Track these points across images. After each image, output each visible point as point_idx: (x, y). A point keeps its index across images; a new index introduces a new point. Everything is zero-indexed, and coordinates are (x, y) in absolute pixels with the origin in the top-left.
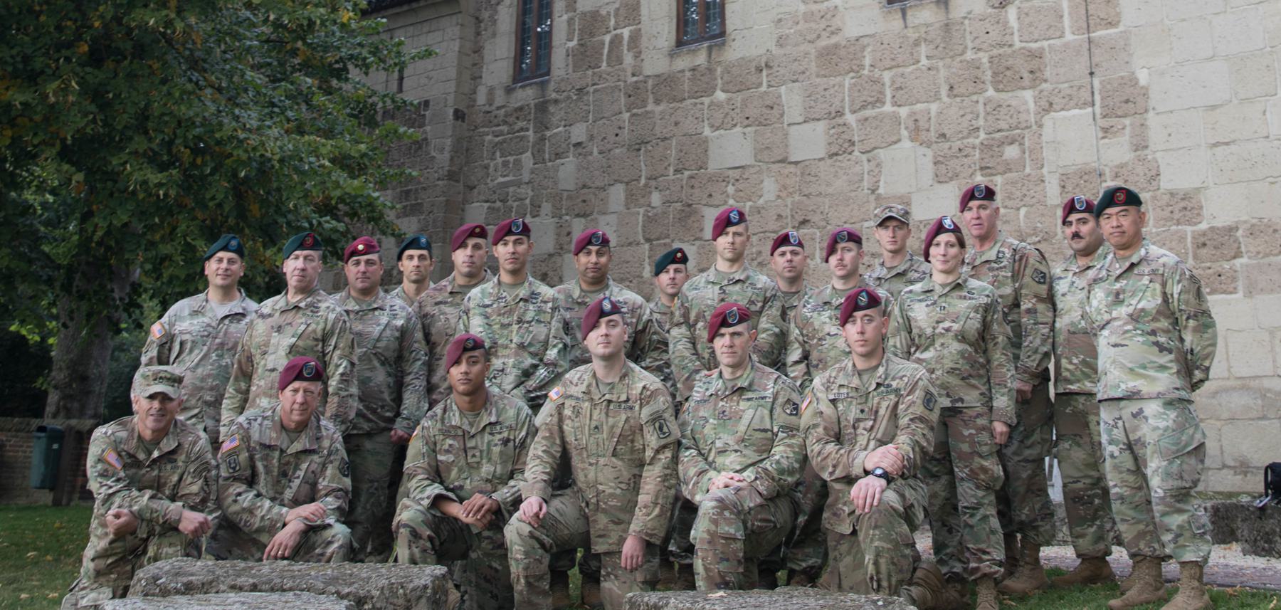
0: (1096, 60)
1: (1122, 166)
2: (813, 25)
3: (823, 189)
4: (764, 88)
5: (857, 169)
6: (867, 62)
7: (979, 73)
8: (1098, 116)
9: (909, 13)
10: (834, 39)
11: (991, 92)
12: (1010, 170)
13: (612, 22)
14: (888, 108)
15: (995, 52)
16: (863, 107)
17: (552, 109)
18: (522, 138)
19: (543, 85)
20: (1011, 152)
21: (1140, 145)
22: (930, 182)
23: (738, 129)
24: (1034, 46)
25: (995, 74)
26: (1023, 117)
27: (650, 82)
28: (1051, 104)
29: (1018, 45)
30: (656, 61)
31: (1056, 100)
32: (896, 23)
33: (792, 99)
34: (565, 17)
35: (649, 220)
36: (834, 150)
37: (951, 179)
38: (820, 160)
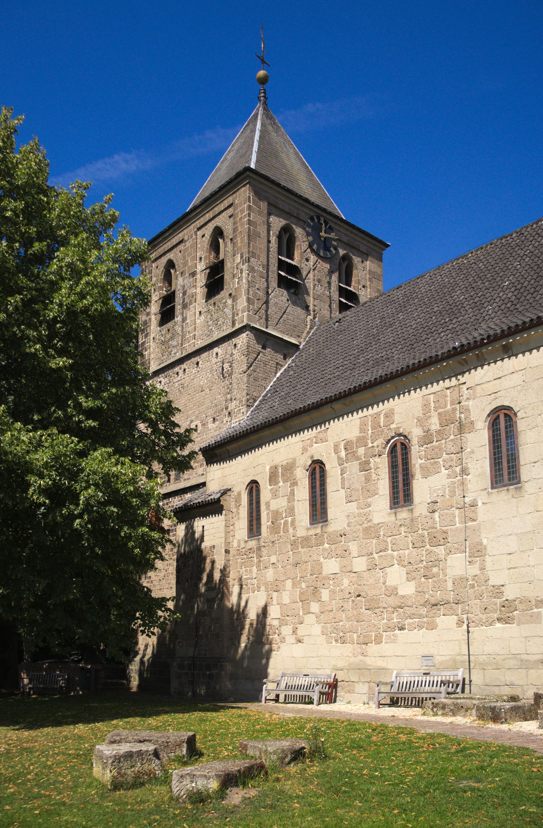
0: (467, 534)
1: (476, 576)
3: (365, 583)
4: (343, 543)
5: (378, 575)
6: (382, 533)
8: (467, 557)
10: (369, 524)
11: (428, 546)
13: (284, 515)
14: (390, 552)
15: (430, 531)
16: (381, 551)
17: (263, 549)
18: (252, 561)
19: (259, 539)
20: (435, 570)
21: (482, 569)
23: (333, 559)
24: (444, 528)
25: (430, 539)
26: (440, 556)
27: (300, 540)
29: (439, 528)
30: (301, 533)
31: (452, 550)
32: (393, 518)
34: (266, 512)
35: (301, 594)
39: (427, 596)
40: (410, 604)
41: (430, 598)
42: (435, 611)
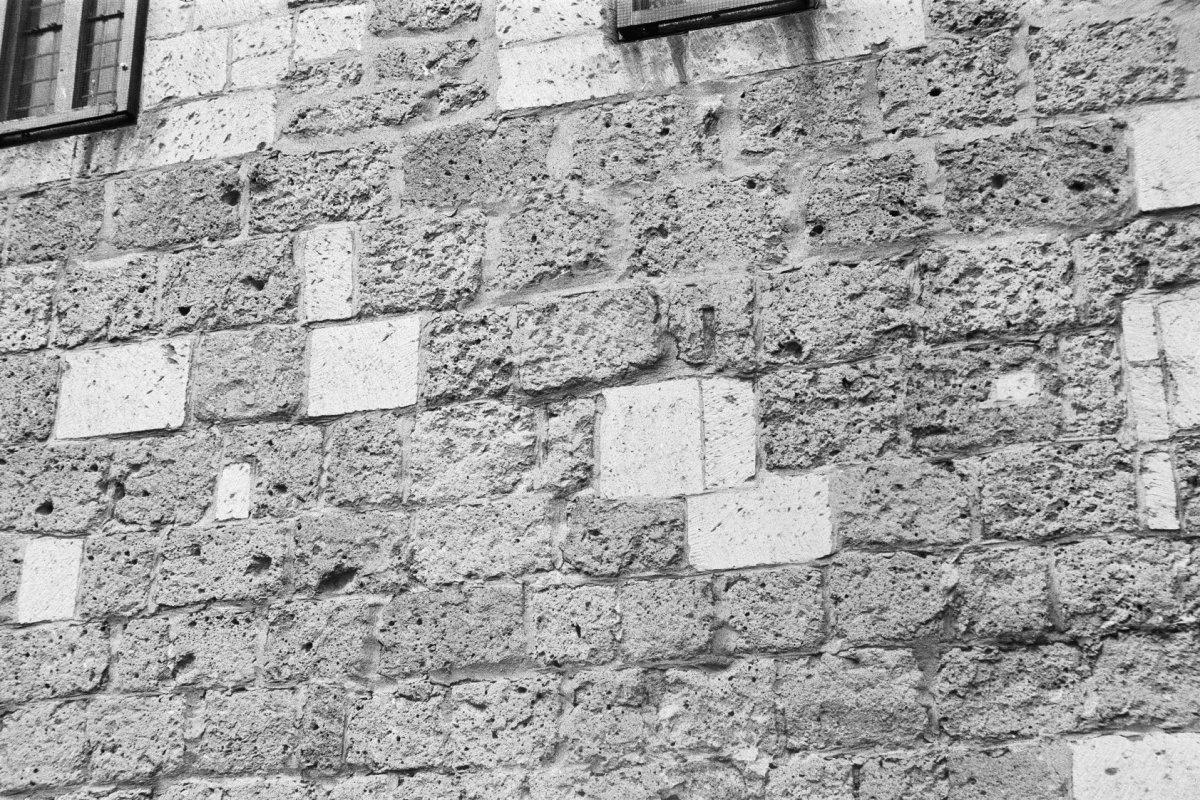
2: (403, 85)
7: (910, 192)
9: (691, 60)
10: (466, 116)
12: (1011, 436)
22: (751, 468)
28: (1143, 265)
33: (330, 266)
36: (443, 386)
37: (818, 460)
38: (398, 412)
39: (951, 575)
40: (795, 631)
41: (976, 587)
42: (1022, 689)
